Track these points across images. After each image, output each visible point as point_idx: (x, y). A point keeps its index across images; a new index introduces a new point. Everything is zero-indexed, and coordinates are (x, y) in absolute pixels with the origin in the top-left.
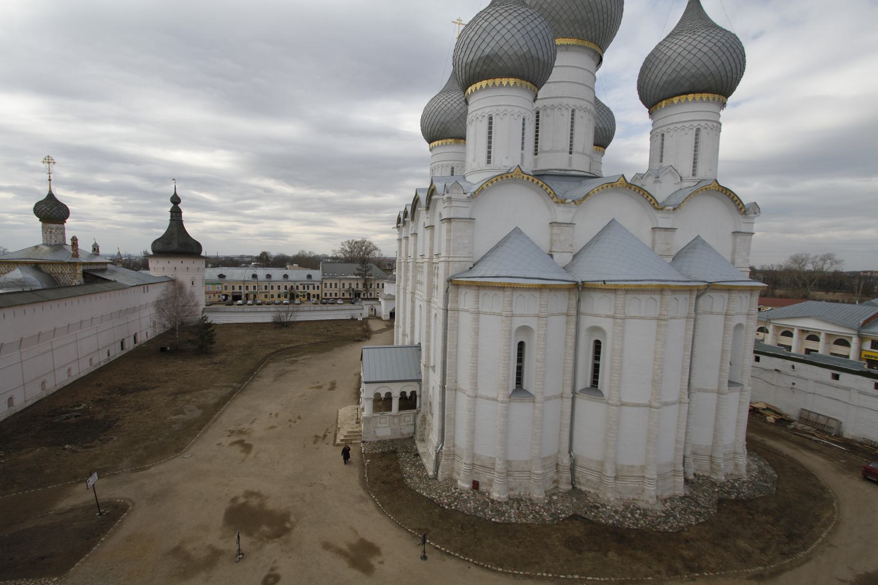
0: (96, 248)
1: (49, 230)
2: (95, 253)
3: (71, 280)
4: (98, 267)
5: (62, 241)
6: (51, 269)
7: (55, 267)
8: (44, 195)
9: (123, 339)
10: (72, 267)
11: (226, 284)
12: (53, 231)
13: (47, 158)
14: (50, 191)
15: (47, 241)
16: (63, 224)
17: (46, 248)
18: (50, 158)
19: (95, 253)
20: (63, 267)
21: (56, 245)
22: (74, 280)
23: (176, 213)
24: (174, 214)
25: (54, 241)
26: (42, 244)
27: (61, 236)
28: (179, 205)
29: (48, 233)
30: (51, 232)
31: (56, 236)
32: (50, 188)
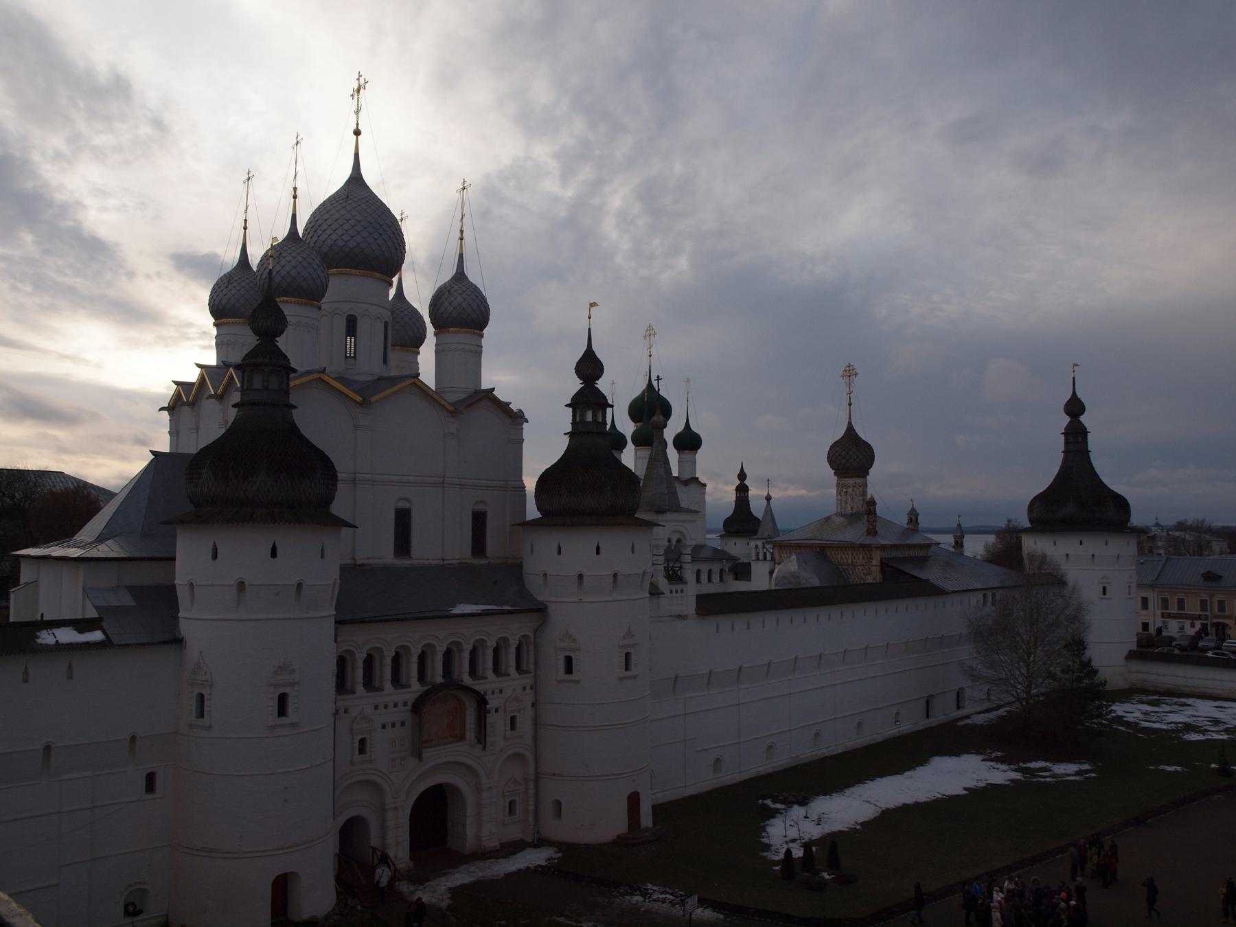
0: (913, 517)
1: (845, 490)
2: (911, 526)
3: (864, 577)
4: (912, 553)
5: (861, 507)
6: (839, 557)
7: (844, 554)
8: (840, 433)
9: (931, 696)
10: (866, 554)
11: (1221, 597)
12: (850, 490)
13: (847, 368)
14: (850, 423)
15: (841, 508)
16: (866, 478)
17: (839, 520)
19: (911, 526)
20: (854, 554)
21: (852, 514)
22: (868, 577)
23: (1076, 436)
24: (1071, 439)
25: (849, 508)
26: (836, 514)
27: (860, 498)
28: (1083, 419)
29: (843, 494)
30: (846, 492)
31: (852, 499)
32: (850, 418)
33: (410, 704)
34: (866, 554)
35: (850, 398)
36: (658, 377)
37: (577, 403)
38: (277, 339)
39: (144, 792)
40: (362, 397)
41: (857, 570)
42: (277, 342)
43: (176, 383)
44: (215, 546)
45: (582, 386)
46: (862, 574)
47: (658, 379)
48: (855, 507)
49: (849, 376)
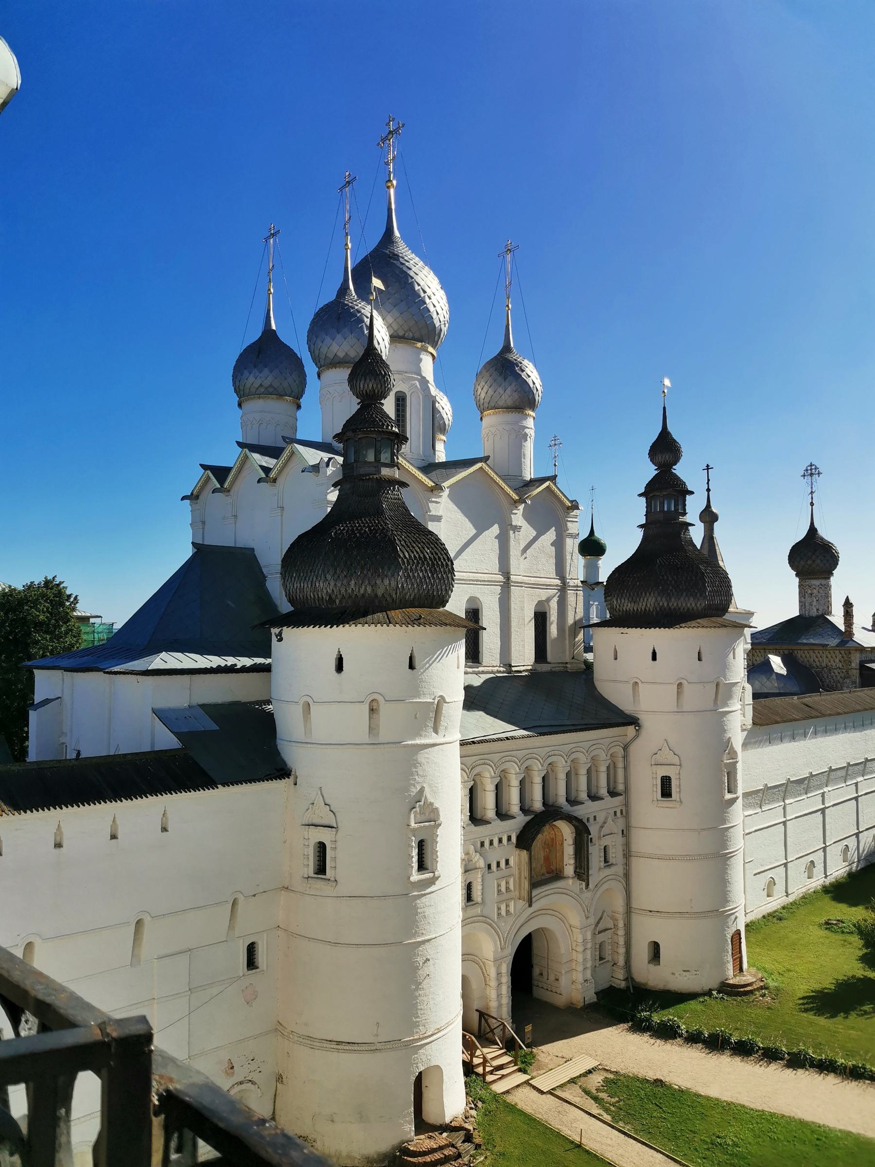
1: (810, 592)
3: (841, 680)
8: (801, 534)
10: (843, 657)
14: (812, 523)
16: (829, 578)
18: (809, 468)
25: (815, 611)
33: (514, 839)
34: (843, 657)
35: (812, 498)
36: (708, 466)
37: (651, 491)
38: (382, 401)
39: (257, 970)
40: (434, 483)
41: (833, 674)
42: (383, 404)
43: (205, 467)
44: (341, 655)
45: (656, 472)
46: (839, 678)
47: (708, 468)
48: (821, 609)
49: (811, 475)
